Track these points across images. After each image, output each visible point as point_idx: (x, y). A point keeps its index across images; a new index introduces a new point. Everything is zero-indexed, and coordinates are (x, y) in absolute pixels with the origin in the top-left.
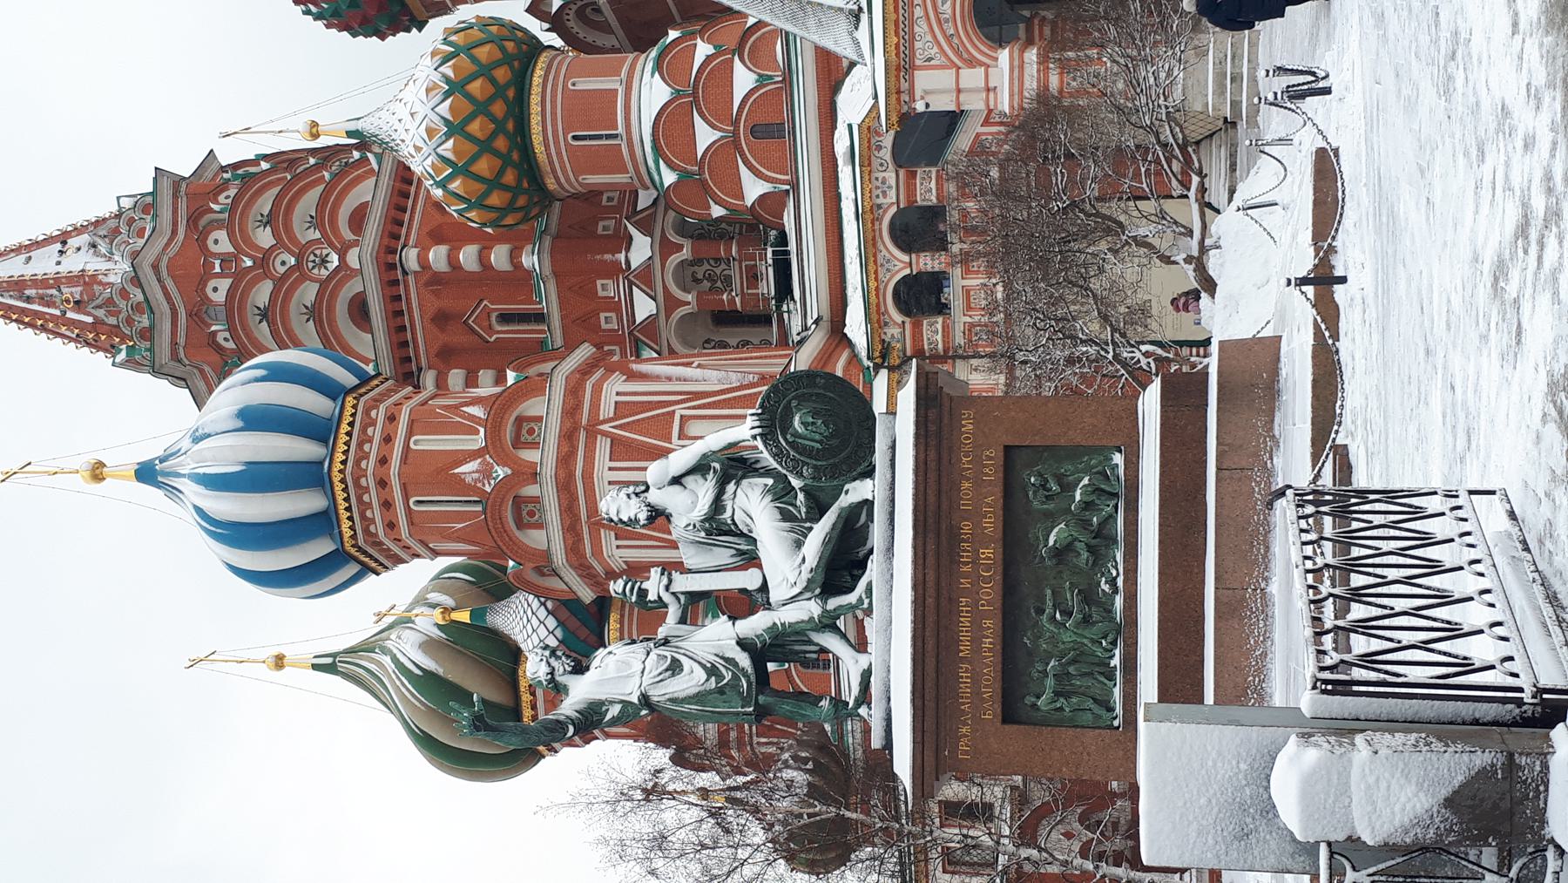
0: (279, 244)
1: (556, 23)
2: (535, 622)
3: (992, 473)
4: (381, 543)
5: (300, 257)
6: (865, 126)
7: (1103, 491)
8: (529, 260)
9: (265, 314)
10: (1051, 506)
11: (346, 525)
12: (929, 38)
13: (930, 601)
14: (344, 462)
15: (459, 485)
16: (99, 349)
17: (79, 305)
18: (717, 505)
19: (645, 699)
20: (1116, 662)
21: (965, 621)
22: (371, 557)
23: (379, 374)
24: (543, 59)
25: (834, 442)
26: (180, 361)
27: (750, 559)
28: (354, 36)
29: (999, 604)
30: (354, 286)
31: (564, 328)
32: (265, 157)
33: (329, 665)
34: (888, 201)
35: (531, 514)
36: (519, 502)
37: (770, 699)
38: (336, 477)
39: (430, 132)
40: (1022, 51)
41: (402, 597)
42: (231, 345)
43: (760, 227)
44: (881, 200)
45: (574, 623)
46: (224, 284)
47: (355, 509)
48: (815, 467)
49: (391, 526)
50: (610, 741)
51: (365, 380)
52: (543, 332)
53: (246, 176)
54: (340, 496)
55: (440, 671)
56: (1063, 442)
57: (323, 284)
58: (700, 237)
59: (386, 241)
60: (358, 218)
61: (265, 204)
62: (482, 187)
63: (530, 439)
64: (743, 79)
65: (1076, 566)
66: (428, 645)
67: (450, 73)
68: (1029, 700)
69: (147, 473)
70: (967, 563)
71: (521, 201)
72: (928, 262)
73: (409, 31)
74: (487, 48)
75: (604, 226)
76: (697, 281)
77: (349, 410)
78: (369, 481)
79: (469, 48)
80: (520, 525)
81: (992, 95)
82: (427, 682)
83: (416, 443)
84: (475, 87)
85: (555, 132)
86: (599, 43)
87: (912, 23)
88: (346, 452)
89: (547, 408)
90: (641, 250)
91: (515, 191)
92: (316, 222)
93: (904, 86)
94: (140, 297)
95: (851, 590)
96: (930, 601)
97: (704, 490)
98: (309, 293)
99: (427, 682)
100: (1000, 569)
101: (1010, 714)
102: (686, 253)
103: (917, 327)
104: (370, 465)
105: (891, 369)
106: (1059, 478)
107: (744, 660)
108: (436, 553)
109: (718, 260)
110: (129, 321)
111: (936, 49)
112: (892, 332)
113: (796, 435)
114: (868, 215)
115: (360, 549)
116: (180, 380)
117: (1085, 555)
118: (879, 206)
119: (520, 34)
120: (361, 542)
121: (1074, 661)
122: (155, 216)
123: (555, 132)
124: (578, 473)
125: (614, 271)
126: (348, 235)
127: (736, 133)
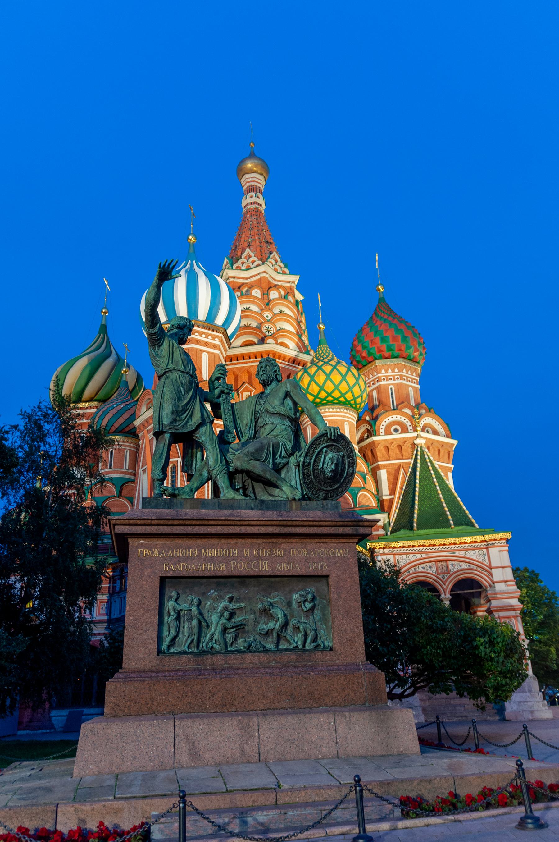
0: (275, 315)
3: (312, 568)
10: (295, 605)
12: (408, 562)
29: (234, 574)
65: (259, 623)
70: (259, 554)
106: (312, 609)
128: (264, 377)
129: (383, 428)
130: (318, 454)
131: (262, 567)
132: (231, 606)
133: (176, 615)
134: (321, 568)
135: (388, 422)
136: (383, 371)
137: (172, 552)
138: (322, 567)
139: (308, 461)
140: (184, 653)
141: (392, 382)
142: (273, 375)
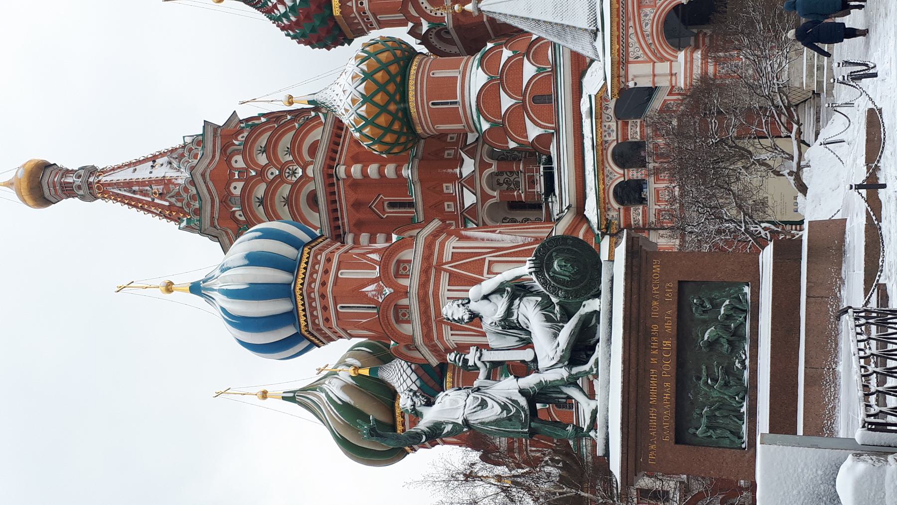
0: (270, 163)
1: (424, 40)
2: (405, 376)
3: (671, 296)
4: (321, 330)
5: (281, 171)
6: (599, 96)
8: (406, 172)
9: (262, 202)
10: (705, 317)
11: (302, 319)
13: (633, 371)
15: (364, 298)
16: (172, 219)
17: (161, 196)
18: (509, 312)
19: (466, 422)
20: (744, 409)
22: (316, 337)
23: (322, 236)
25: (578, 277)
26: (215, 227)
27: (527, 343)
29: (674, 374)
30: (310, 187)
31: (424, 210)
32: (264, 115)
33: (291, 397)
34: (611, 138)
35: (404, 315)
36: (397, 308)
37: (538, 425)
38: (298, 292)
39: (354, 101)
40: (692, 52)
41: (332, 360)
42: (243, 218)
43: (537, 154)
44: (607, 138)
45: (427, 377)
46: (240, 185)
47: (307, 310)
48: (566, 291)
49: (327, 320)
50: (445, 446)
51: (315, 238)
52: (413, 213)
53: (253, 125)
54: (300, 303)
55: (352, 403)
56: (713, 279)
57: (294, 185)
58: (503, 159)
59: (328, 162)
60: (313, 149)
61: (263, 141)
62: (381, 132)
63: (404, 272)
64: (529, 70)
65: (721, 353)
66: (346, 388)
67: (365, 68)
68: (692, 431)
69: (196, 288)
70: (655, 349)
71: (402, 140)
72: (634, 174)
73: (343, 45)
74: (385, 54)
75: (448, 153)
76: (499, 184)
77: (306, 255)
79: (376, 54)
80: (398, 321)
81: (674, 78)
82: (345, 408)
83: (342, 274)
84: (379, 76)
85: (422, 100)
86: (448, 51)
87: (628, 36)
88: (303, 279)
89: (414, 255)
90: (468, 166)
91: (399, 133)
92: (291, 151)
93: (622, 73)
94: (195, 192)
95: (586, 363)
96: (633, 371)
97: (501, 304)
98: (285, 190)
99: (345, 408)
100: (675, 353)
101: (680, 438)
102: (494, 169)
103: (627, 211)
104: (316, 286)
105: (611, 235)
107: (523, 402)
108: (351, 336)
110: (188, 205)
111: (641, 52)
112: (613, 214)
113: (555, 272)
114: (600, 147)
115: (310, 333)
116: (214, 237)
117: (727, 346)
118: (606, 142)
119: (404, 46)
120: (310, 329)
121: (718, 409)
122: (204, 147)
123: (422, 100)
124: (431, 292)
125: (453, 178)
126: (307, 158)
127: (524, 101)
130: (554, 281)
134: (671, 289)
138: (670, 288)
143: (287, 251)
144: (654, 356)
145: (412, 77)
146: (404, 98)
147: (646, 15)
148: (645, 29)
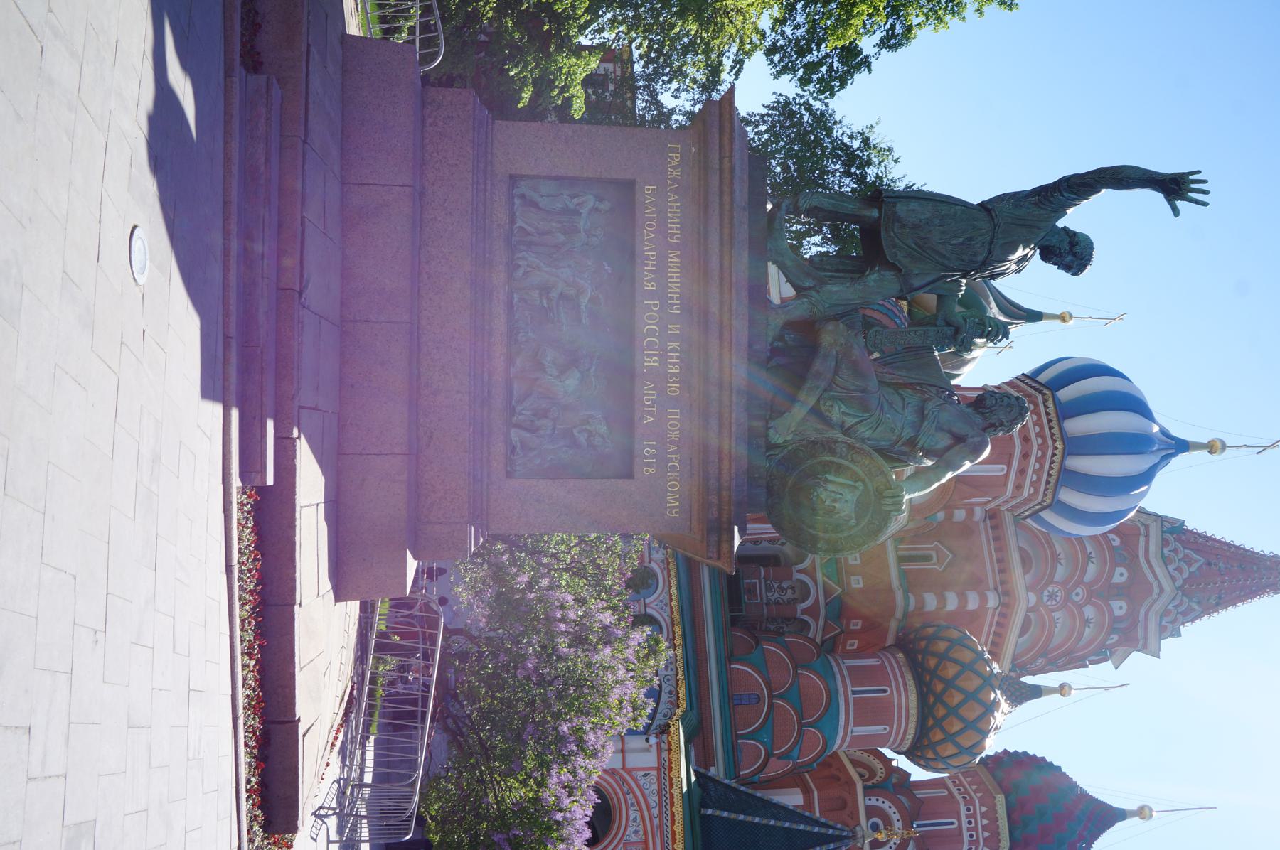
0: (1080, 607)
7: (526, 429)
12: (647, 792)
14: (1054, 455)
21: (674, 289)
24: (905, 747)
28: (1025, 753)
38: (1059, 445)
42: (1111, 536)
46: (1117, 579)
47: (1045, 421)
51: (1035, 515)
53: (1099, 654)
54: (1056, 430)
57: (1051, 581)
58: (789, 619)
69: (1183, 446)
70: (673, 350)
71: (923, 644)
76: (792, 588)
78: (1035, 441)
88: (1052, 462)
93: (665, 755)
95: (789, 325)
98: (1061, 572)
104: (1035, 453)
109: (777, 603)
110: (1175, 551)
120: (1040, 398)
127: (771, 697)
128: (989, 402)
129: (879, 804)
131: (650, 356)
132: (584, 301)
133: (571, 206)
135: (891, 811)
136: (984, 809)
137: (676, 201)
138: (648, 465)
139: (838, 450)
140: (513, 221)
141: (965, 826)
142: (994, 420)
143: (1070, 497)
144: (673, 338)
145: (912, 725)
146: (922, 698)
147: (636, 832)
148: (638, 814)
